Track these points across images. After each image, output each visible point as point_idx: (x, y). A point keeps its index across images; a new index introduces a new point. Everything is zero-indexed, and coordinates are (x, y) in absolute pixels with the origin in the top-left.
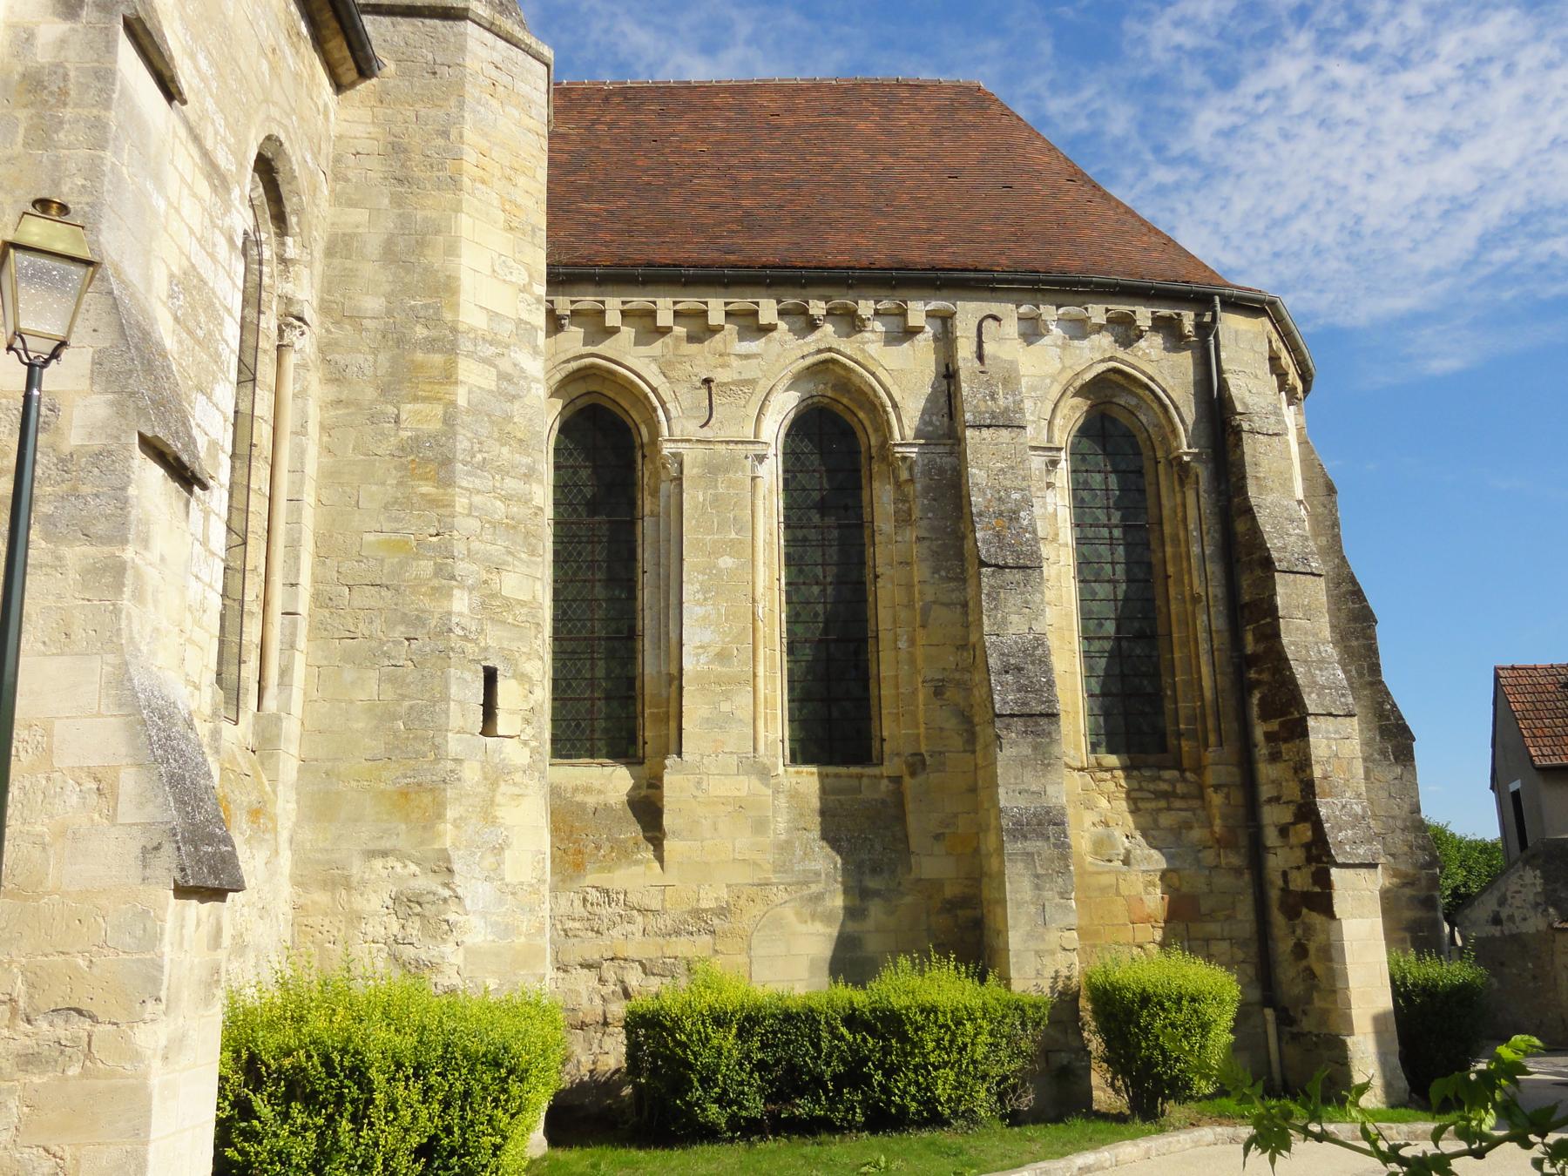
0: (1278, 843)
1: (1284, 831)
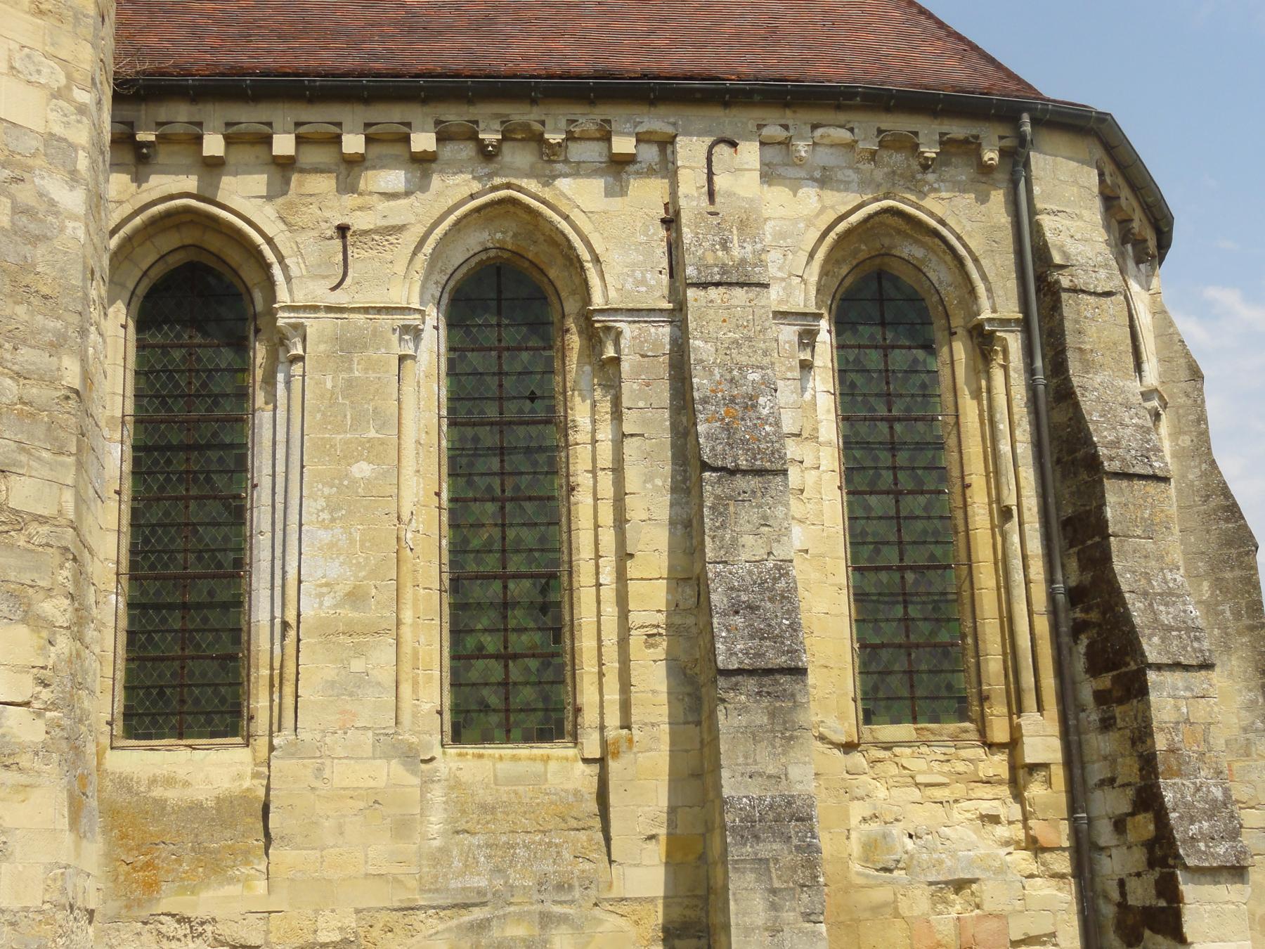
0: (1114, 842)
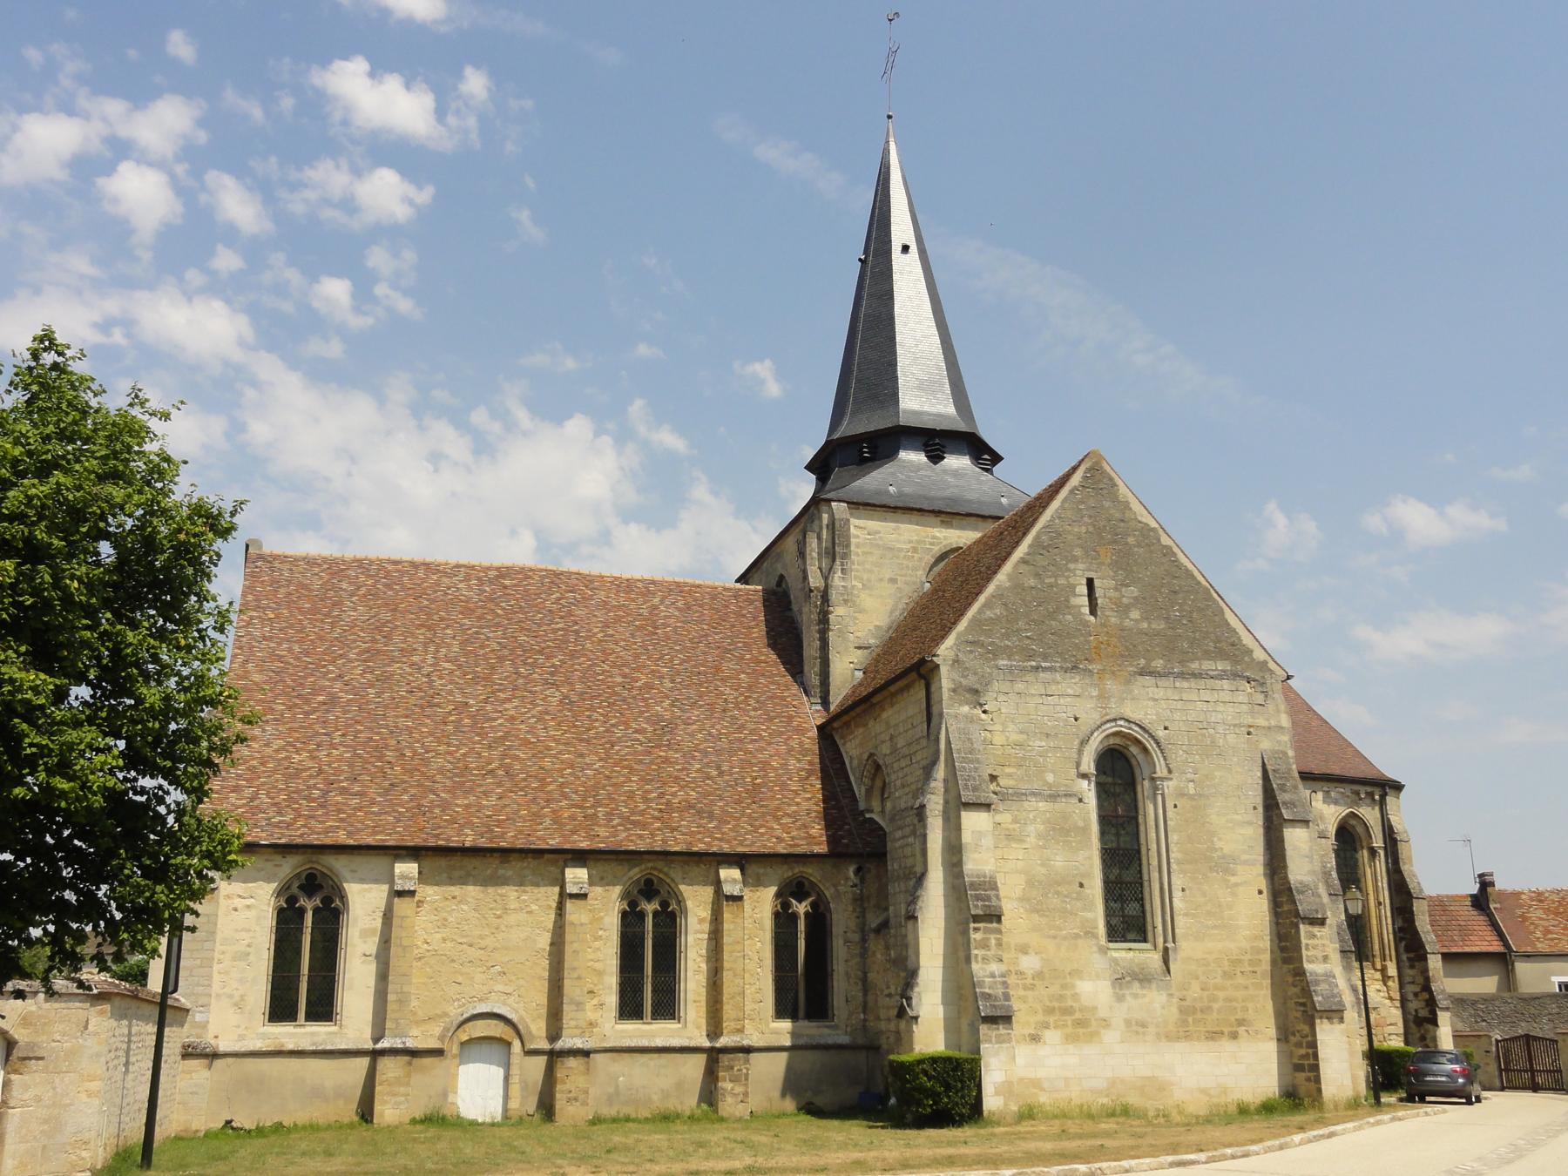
1: (1416, 995)
